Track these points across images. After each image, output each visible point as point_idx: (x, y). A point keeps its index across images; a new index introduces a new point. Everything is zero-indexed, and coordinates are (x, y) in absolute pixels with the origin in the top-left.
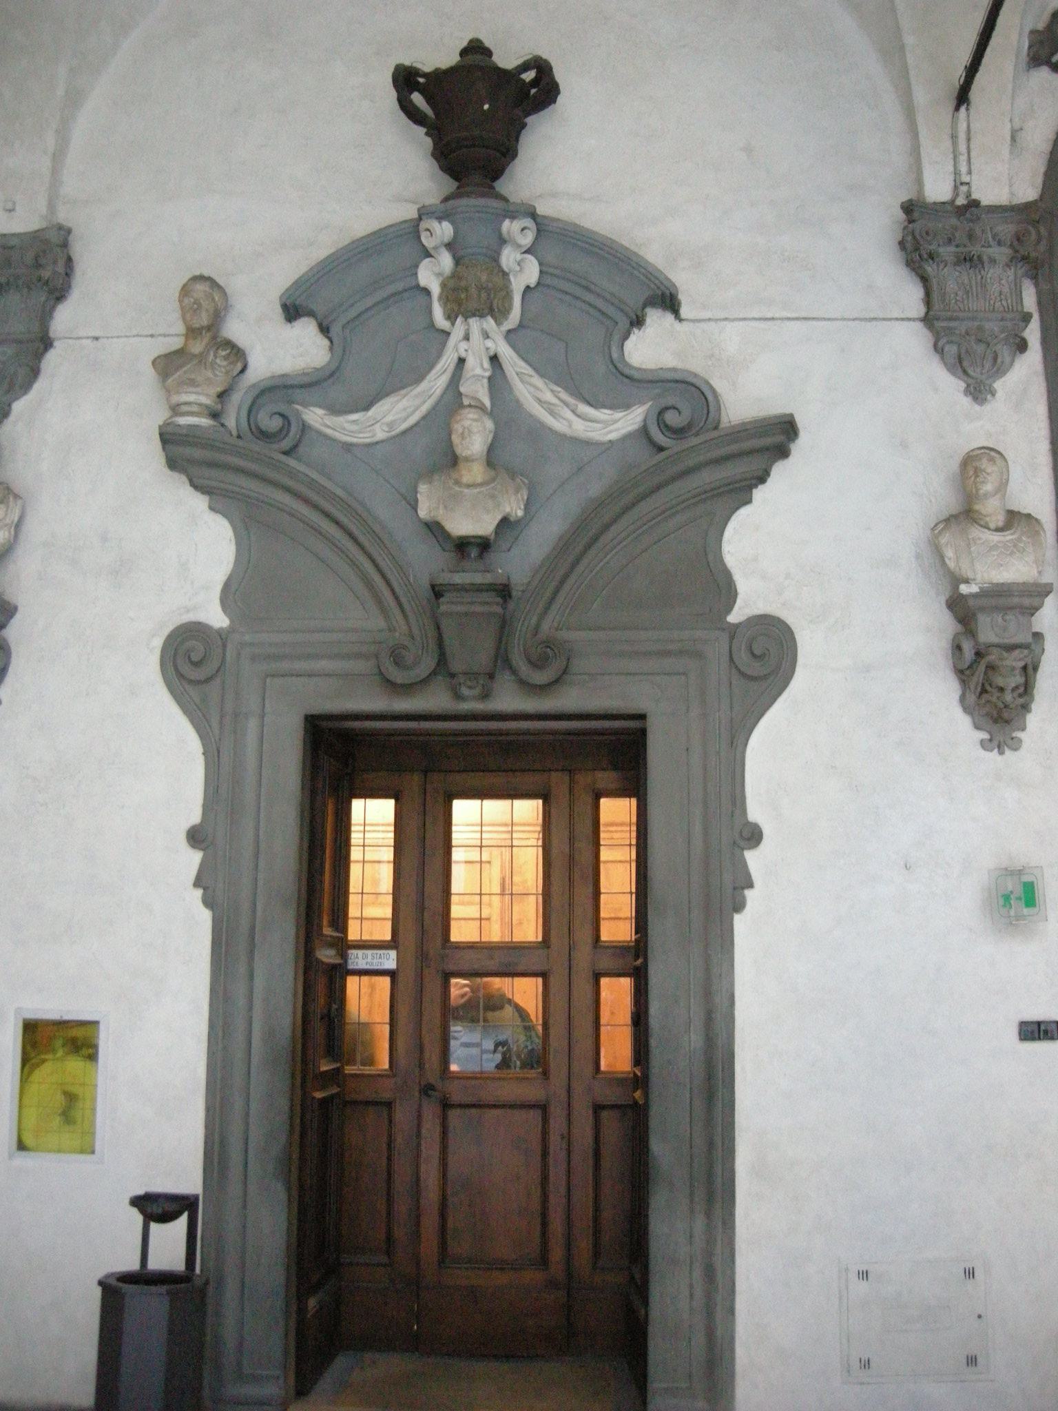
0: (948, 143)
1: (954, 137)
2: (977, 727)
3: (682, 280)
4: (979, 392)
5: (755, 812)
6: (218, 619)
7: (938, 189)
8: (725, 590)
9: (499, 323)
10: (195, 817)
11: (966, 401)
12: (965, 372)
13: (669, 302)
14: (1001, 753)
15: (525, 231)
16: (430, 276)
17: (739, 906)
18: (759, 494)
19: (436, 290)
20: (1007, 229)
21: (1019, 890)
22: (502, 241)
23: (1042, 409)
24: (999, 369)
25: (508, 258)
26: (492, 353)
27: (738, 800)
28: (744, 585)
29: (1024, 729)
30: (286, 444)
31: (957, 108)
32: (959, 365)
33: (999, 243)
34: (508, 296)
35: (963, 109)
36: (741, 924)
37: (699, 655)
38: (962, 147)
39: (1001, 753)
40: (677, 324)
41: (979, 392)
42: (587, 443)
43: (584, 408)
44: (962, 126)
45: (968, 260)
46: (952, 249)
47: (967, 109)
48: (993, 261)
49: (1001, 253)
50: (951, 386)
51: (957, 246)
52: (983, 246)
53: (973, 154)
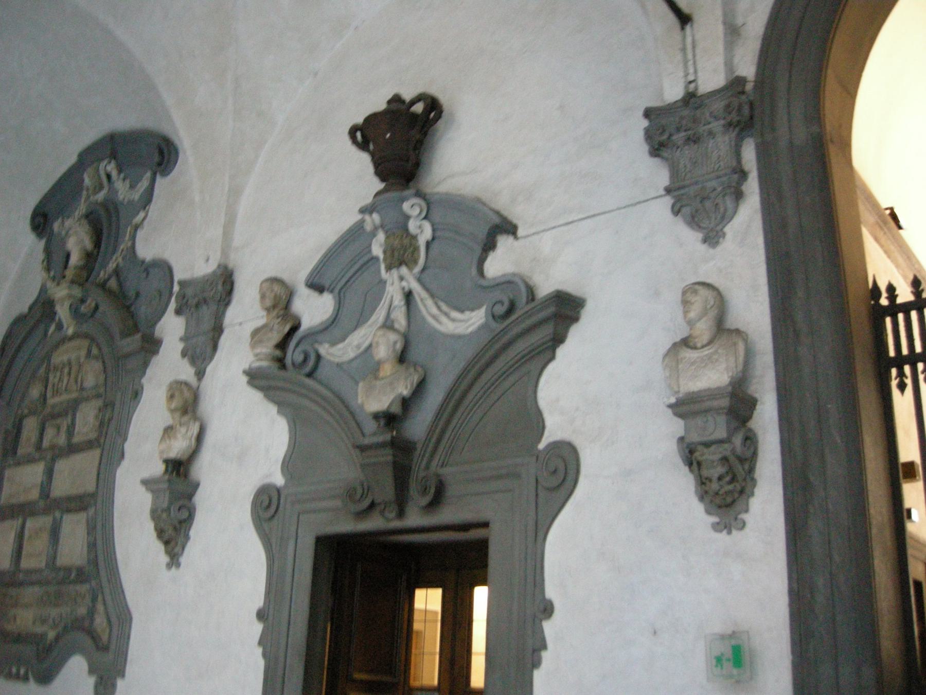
0: (679, 57)
1: (684, 50)
2: (708, 512)
3: (517, 213)
4: (712, 238)
5: (551, 591)
6: (279, 480)
7: (673, 92)
8: (539, 426)
9: (410, 269)
10: (259, 602)
11: (703, 248)
12: (700, 227)
13: (509, 228)
14: (729, 533)
15: (414, 207)
16: (377, 250)
17: (536, 664)
18: (561, 351)
19: (381, 256)
20: (718, 106)
21: (728, 653)
22: (407, 218)
23: (760, 240)
24: (726, 218)
25: (412, 226)
26: (407, 289)
27: (539, 582)
28: (550, 421)
29: (747, 511)
30: (308, 369)
31: (683, 28)
32: (693, 222)
33: (716, 118)
34: (416, 249)
35: (688, 28)
36: (538, 676)
37: (518, 476)
38: (690, 56)
39: (729, 533)
40: (516, 243)
41: (712, 238)
42: (459, 337)
43: (455, 314)
44: (689, 40)
45: (694, 140)
46: (683, 134)
47: (692, 26)
48: (711, 134)
49: (717, 126)
50: (692, 238)
51: (686, 131)
52: (704, 125)
53: (698, 57)
